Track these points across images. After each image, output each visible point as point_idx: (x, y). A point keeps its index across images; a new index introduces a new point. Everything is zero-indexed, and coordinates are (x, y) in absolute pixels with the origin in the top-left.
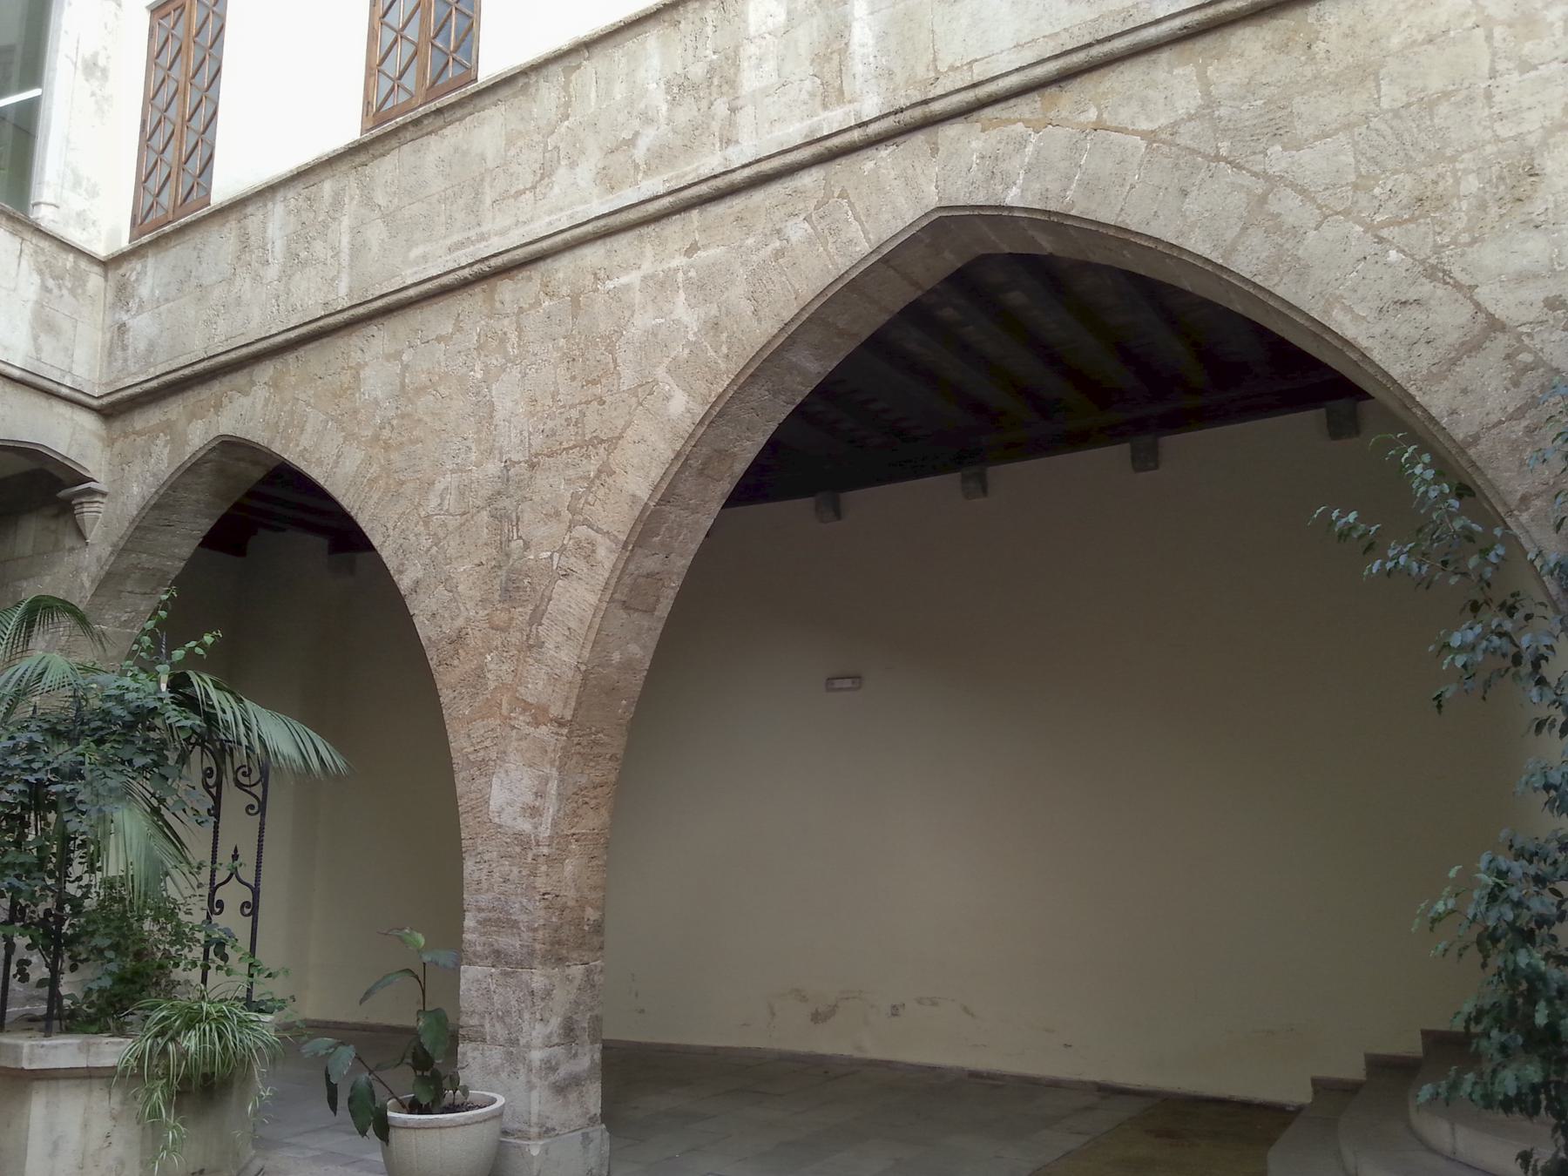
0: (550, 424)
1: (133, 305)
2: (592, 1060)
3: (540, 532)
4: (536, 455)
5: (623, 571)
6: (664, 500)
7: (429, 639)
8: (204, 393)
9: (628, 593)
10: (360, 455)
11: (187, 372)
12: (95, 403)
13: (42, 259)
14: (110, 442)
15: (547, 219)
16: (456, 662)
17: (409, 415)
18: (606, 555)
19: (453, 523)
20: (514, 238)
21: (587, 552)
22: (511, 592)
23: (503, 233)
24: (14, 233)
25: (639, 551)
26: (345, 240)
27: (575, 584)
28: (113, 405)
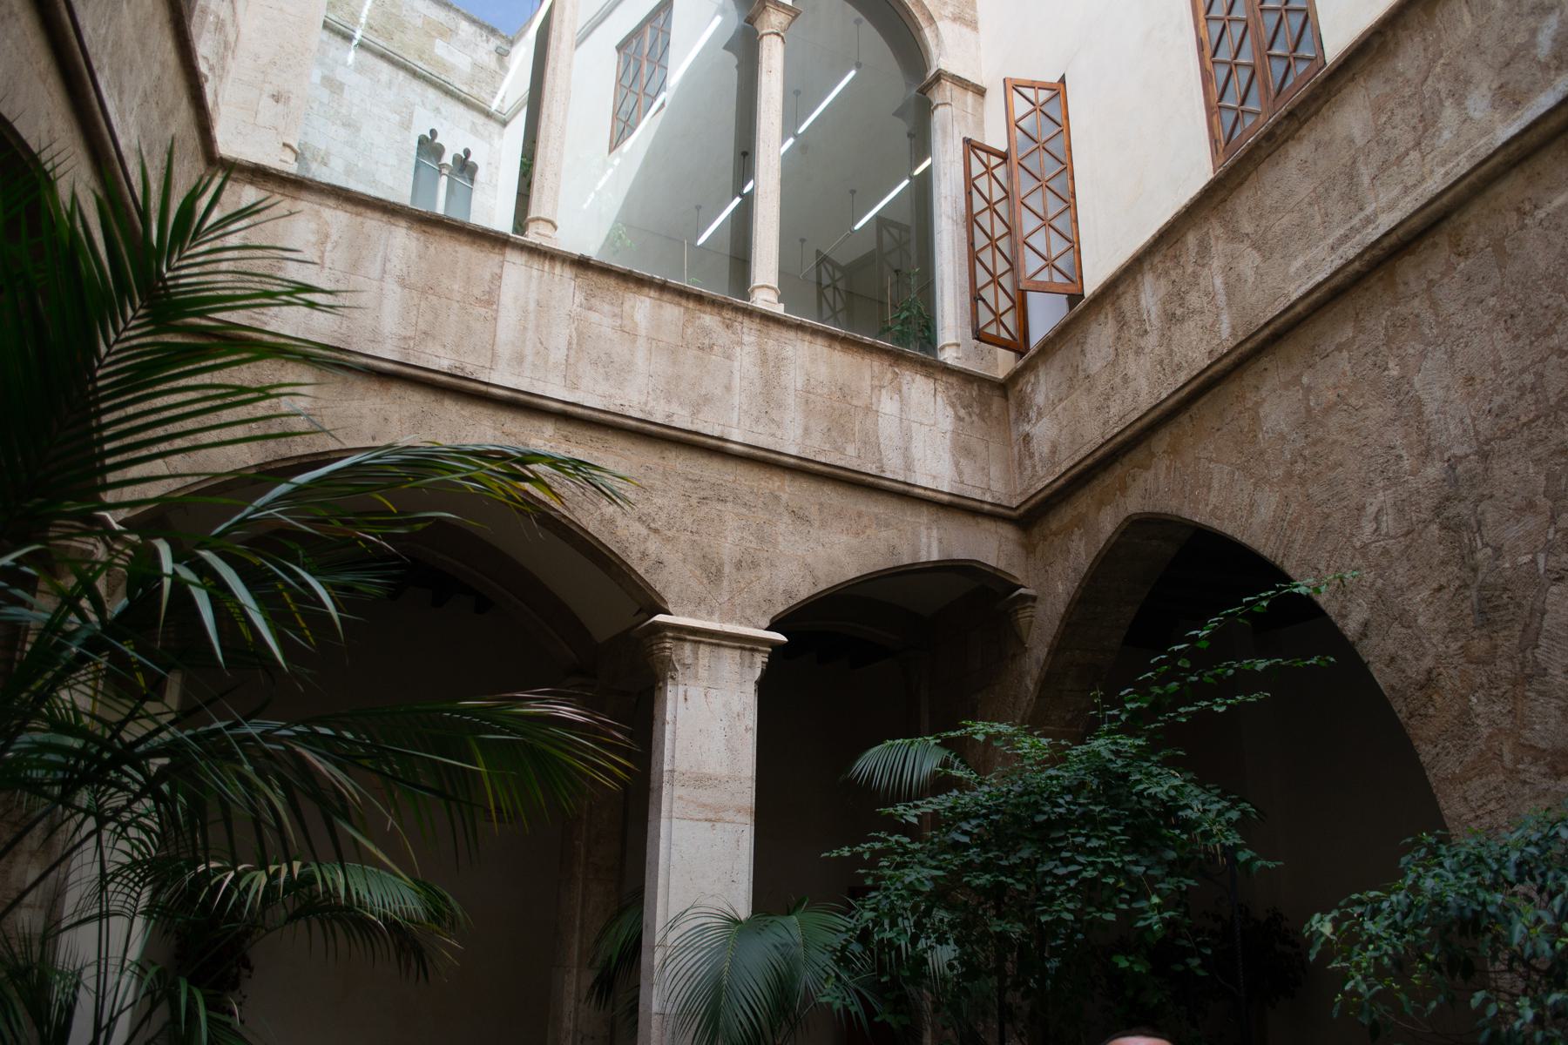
0: (1498, 400)
1: (1033, 414)
3: (1512, 533)
4: (1488, 442)
7: (1392, 688)
8: (1109, 479)
10: (1275, 499)
11: (1089, 461)
13: (952, 393)
14: (1029, 549)
15: (1443, 171)
16: (1431, 711)
17: (1321, 440)
19: (1395, 547)
20: (1408, 206)
22: (1489, 611)
23: (1391, 207)
24: (928, 376)
26: (1218, 281)
28: (1028, 511)
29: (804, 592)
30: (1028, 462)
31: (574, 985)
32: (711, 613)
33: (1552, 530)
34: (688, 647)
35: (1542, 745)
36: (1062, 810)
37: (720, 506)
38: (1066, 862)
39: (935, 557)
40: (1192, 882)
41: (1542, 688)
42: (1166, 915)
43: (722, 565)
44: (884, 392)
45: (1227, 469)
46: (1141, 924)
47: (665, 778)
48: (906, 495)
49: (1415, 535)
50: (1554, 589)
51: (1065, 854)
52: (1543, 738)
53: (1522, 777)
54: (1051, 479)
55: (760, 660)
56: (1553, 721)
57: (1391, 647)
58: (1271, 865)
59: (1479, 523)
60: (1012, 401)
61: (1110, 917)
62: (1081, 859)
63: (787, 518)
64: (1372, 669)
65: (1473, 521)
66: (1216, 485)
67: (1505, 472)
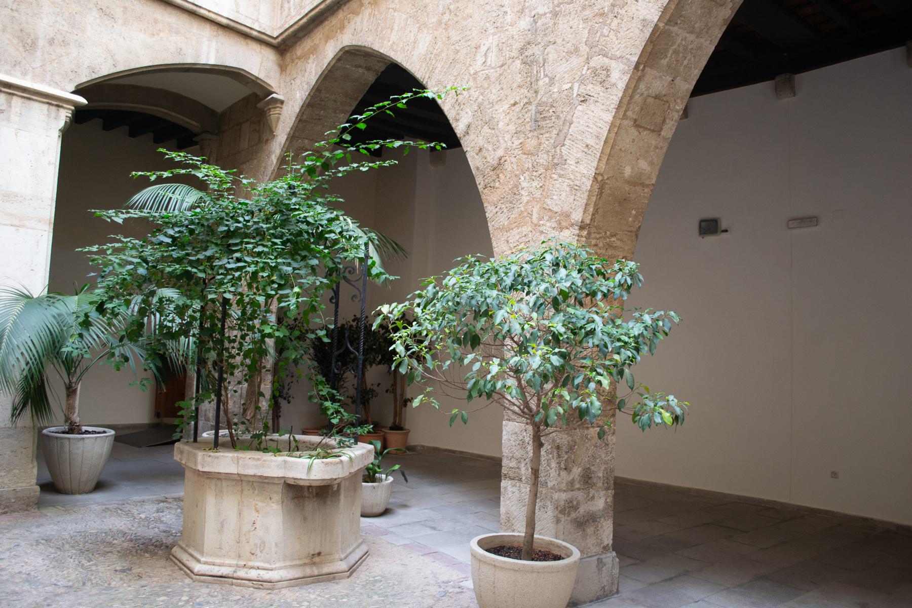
2: (606, 502)
4: (558, 6)
5: (634, 91)
6: (671, 21)
7: (478, 168)
8: (334, 21)
9: (636, 111)
12: (274, 42)
14: (283, 68)
16: (497, 184)
18: (620, 77)
19: (493, 74)
21: (601, 76)
22: (539, 122)
25: (648, 70)
27: (592, 107)
28: (284, 41)
29: (105, 69)
30: (286, 6)
32: (24, 74)
33: (586, 68)
35: (556, 209)
36: (240, 225)
38: (238, 260)
39: (212, 61)
41: (562, 172)
43: (37, 39)
45: (404, 16)
49: (506, 67)
50: (580, 108)
51: (238, 255)
52: (556, 205)
53: (541, 229)
55: (64, 116)
56: (564, 194)
57: (481, 142)
58: (392, 278)
59: (544, 60)
62: (248, 259)
63: (95, 13)
64: (468, 156)
65: (541, 60)
66: (396, 28)
67: (566, 26)
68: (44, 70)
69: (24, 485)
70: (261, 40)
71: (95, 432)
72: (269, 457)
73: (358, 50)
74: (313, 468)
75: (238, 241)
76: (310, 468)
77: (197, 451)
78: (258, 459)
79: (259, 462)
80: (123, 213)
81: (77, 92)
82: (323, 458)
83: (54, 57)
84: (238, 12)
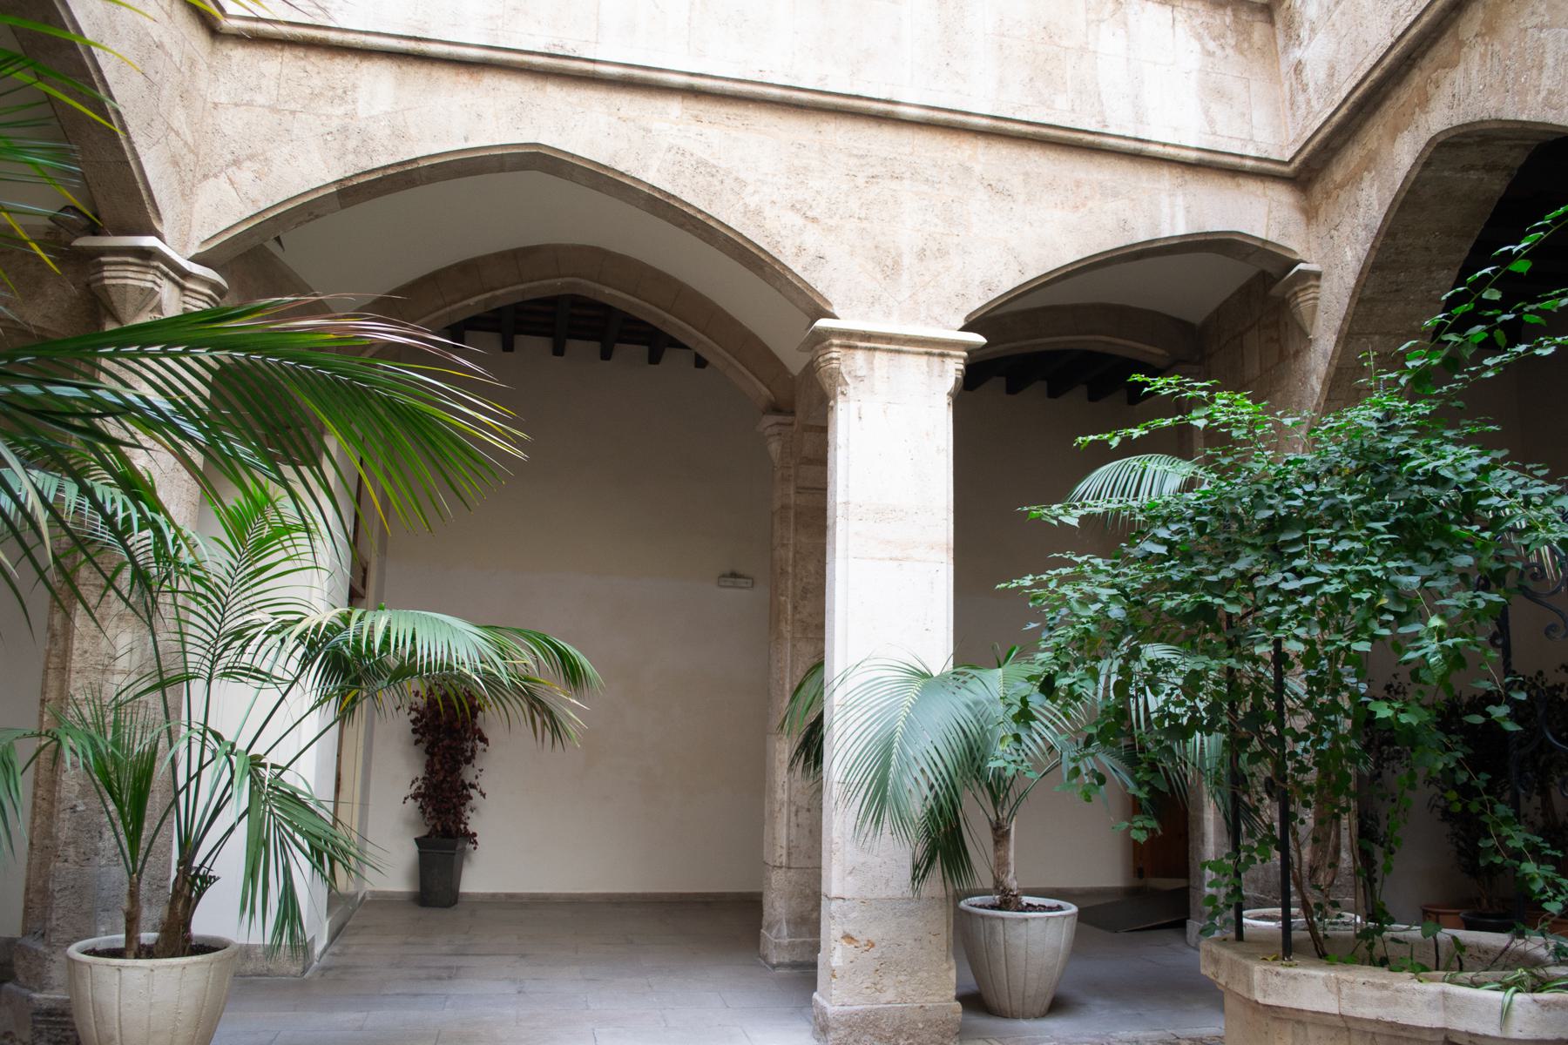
1: (1304, 33)
8: (1404, 95)
11: (1376, 74)
13: (1197, 21)
14: (1310, 214)
28: (1306, 163)
29: (1008, 281)
30: (1301, 98)
31: (784, 748)
32: (888, 314)
34: (859, 355)
36: (1298, 503)
37: (894, 184)
38: (1300, 575)
39: (1181, 230)
40: (1495, 597)
42: (1449, 642)
43: (900, 255)
44: (1103, 26)
46: (1411, 655)
47: (839, 513)
48: (1138, 156)
54: (1330, 111)
55: (952, 370)
60: (1279, 25)
61: (1363, 646)
66: (1550, 61)
68: (916, 303)
69: (937, 998)
70: (1263, 173)
71: (1043, 908)
72: (1404, 982)
73: (1465, 135)
74: (1514, 1013)
75: (1297, 535)
76: (1506, 1013)
77: (1249, 962)
78: (1384, 987)
79: (1386, 993)
80: (1075, 507)
81: (967, 328)
82: (1533, 991)
83: (927, 278)
84: (1214, 134)
